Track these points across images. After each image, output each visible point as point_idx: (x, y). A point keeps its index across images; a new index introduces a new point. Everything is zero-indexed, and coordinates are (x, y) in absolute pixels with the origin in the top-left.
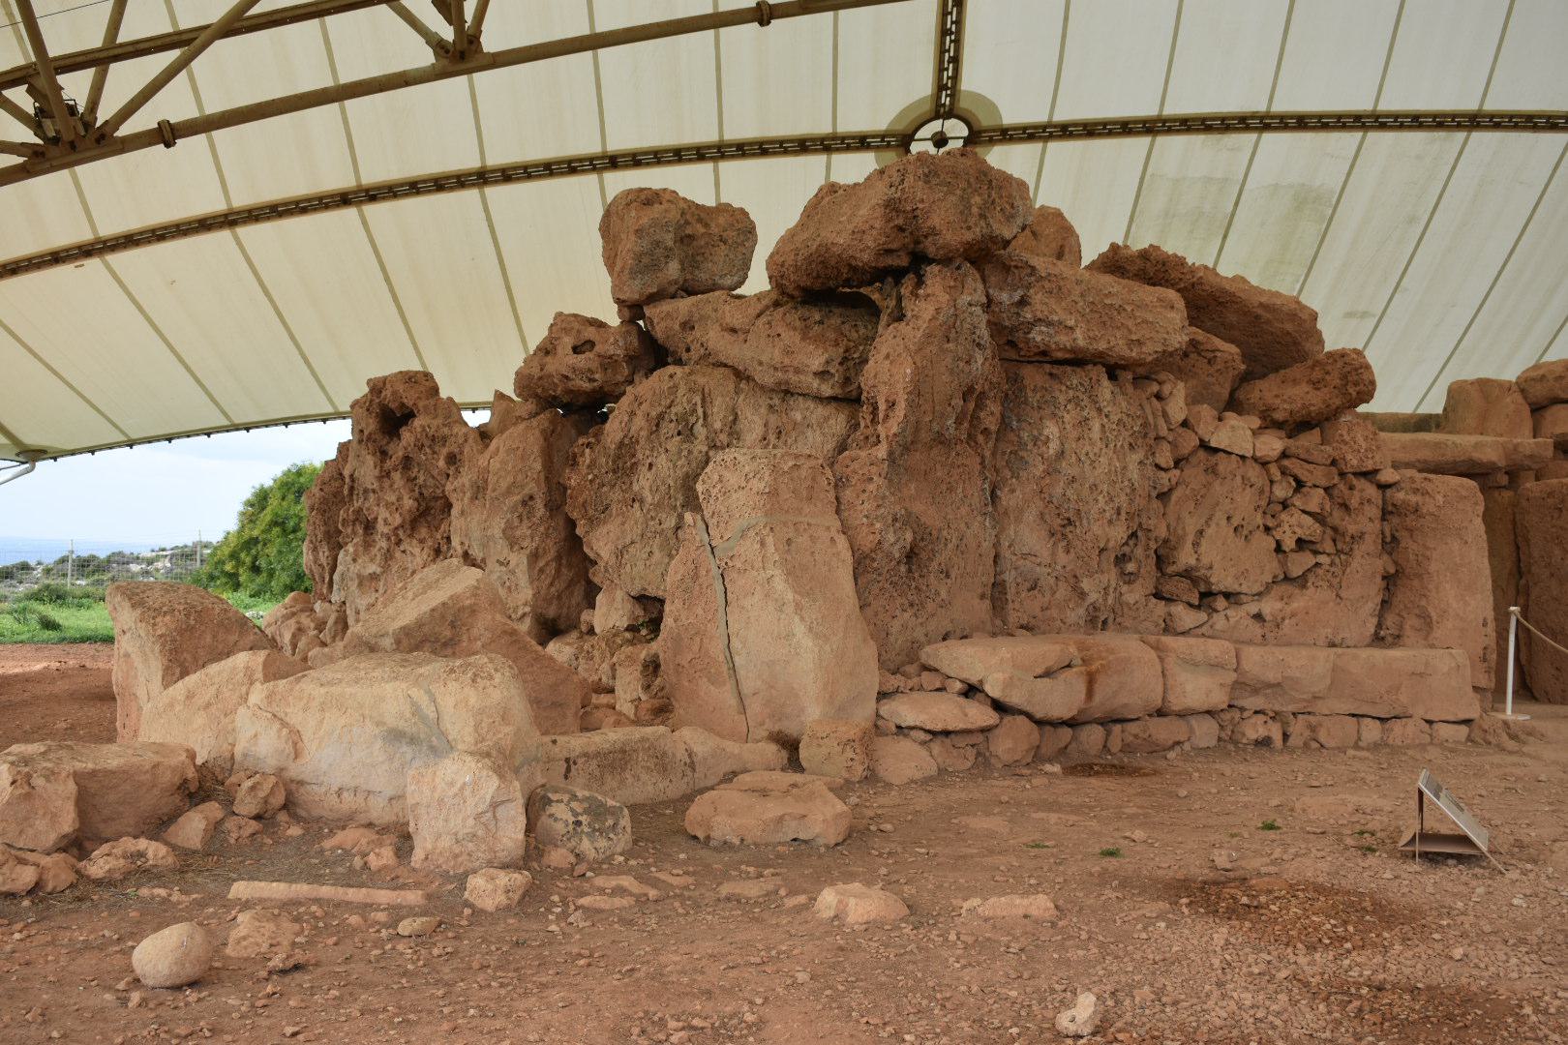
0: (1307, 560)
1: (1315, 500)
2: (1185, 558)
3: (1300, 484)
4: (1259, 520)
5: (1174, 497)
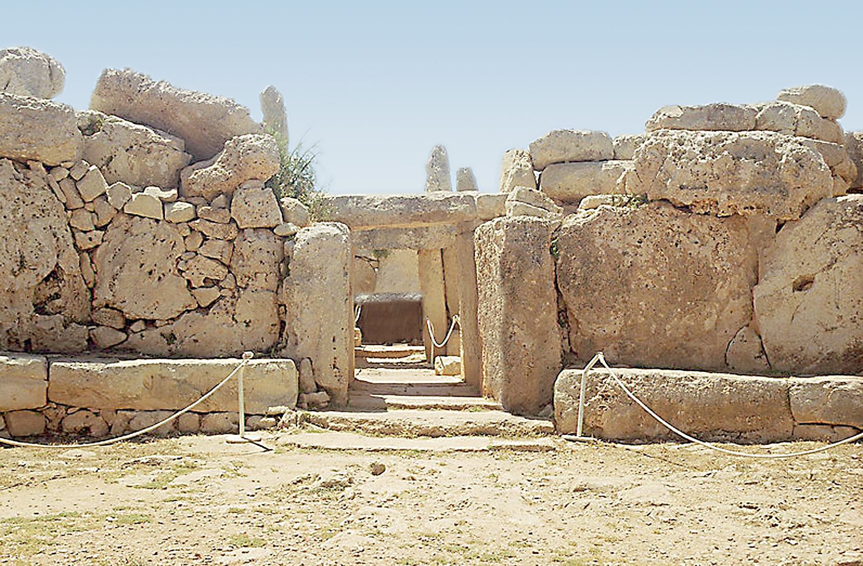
0: (214, 293)
1: (217, 248)
2: (103, 295)
3: (205, 238)
4: (170, 264)
5: (98, 251)
